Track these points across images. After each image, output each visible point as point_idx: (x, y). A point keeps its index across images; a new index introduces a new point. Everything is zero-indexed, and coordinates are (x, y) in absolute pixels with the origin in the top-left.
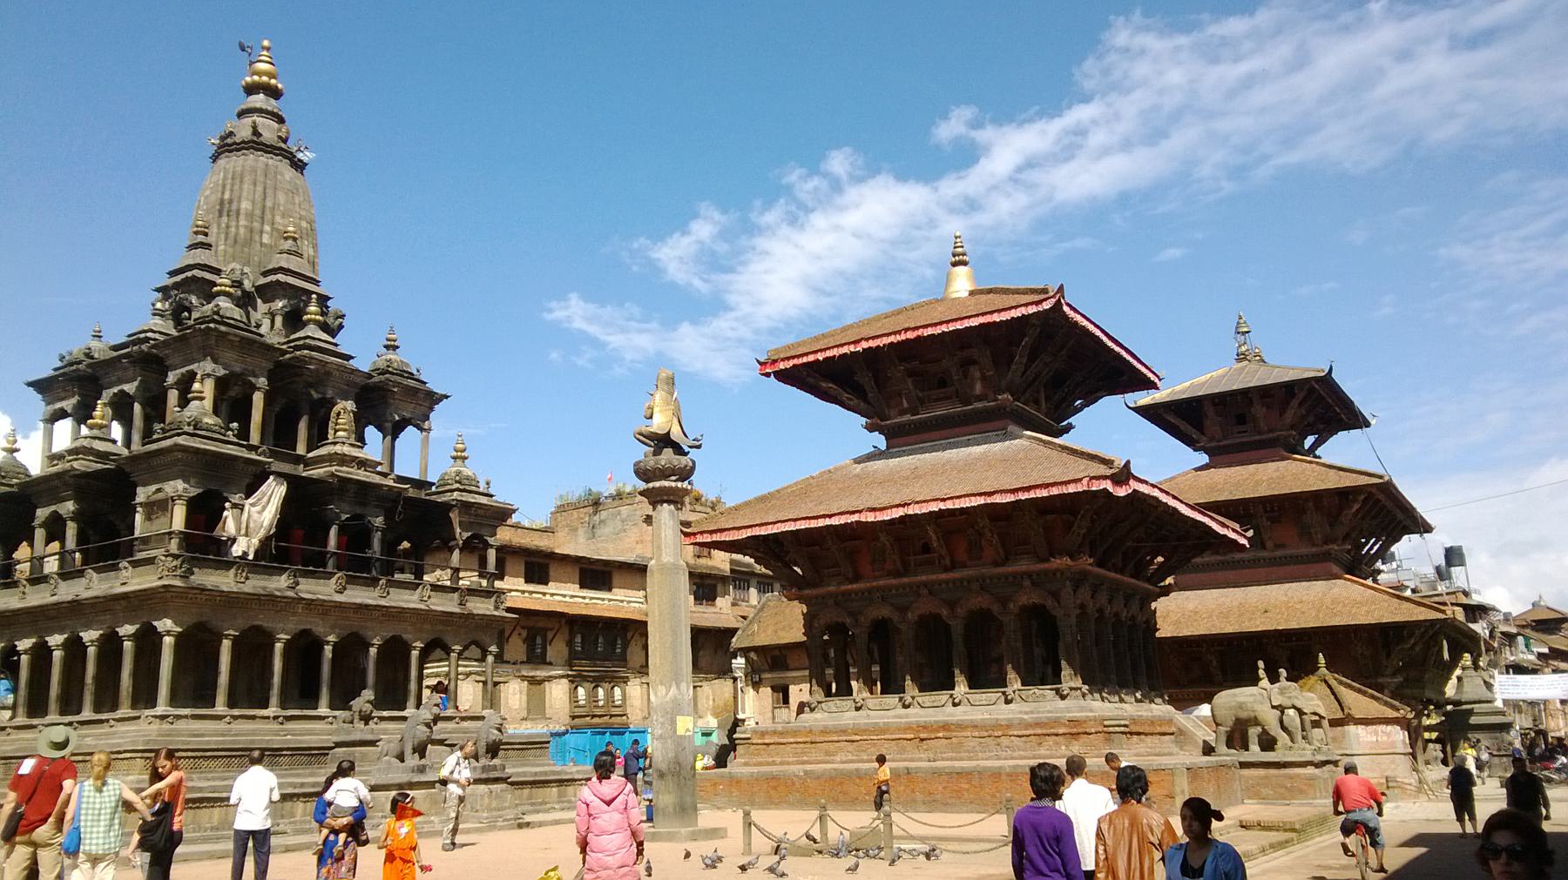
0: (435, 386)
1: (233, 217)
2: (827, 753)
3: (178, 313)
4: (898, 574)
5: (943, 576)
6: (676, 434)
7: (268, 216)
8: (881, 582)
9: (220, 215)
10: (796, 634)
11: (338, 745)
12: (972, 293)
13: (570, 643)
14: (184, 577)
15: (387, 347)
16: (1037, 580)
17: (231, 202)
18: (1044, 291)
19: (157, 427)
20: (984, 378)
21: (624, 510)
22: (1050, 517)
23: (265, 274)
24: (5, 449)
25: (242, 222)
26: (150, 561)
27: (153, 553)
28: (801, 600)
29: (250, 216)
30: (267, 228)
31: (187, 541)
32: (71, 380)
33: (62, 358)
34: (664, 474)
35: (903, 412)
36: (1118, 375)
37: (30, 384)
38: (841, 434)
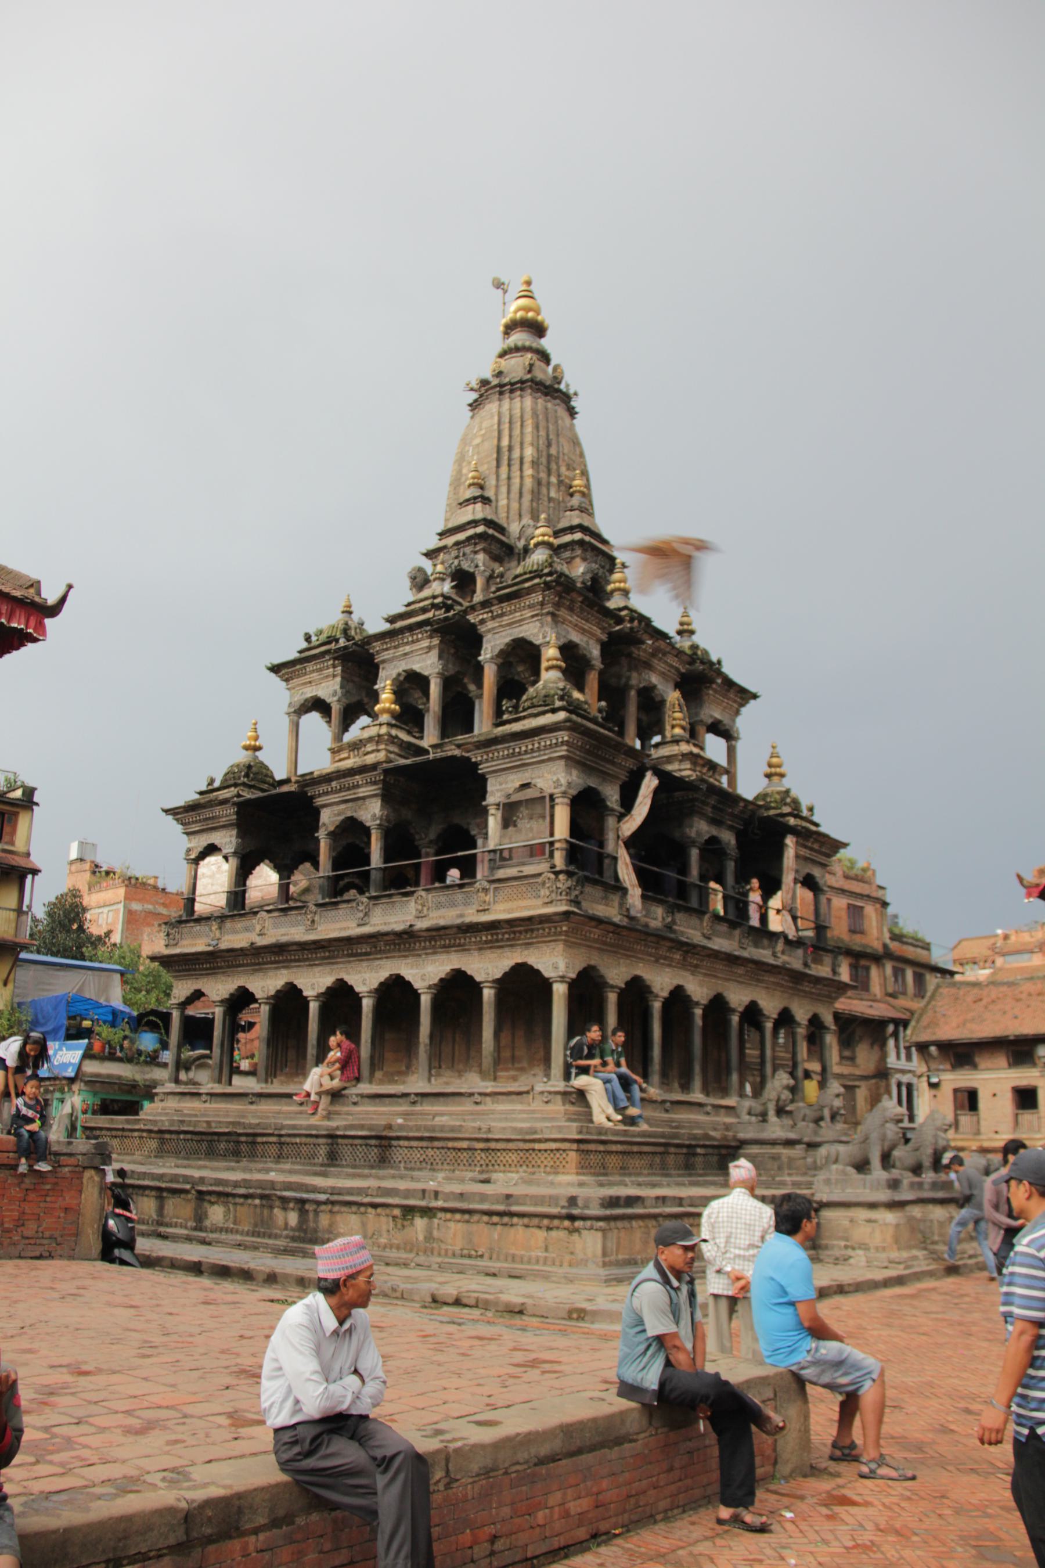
1: (516, 467)
7: (554, 466)
9: (498, 466)
14: (576, 902)
17: (510, 448)
19: (506, 704)
23: (557, 534)
24: (247, 748)
29: (535, 464)
30: (554, 480)
31: (573, 854)
33: (308, 638)
37: (275, 669)
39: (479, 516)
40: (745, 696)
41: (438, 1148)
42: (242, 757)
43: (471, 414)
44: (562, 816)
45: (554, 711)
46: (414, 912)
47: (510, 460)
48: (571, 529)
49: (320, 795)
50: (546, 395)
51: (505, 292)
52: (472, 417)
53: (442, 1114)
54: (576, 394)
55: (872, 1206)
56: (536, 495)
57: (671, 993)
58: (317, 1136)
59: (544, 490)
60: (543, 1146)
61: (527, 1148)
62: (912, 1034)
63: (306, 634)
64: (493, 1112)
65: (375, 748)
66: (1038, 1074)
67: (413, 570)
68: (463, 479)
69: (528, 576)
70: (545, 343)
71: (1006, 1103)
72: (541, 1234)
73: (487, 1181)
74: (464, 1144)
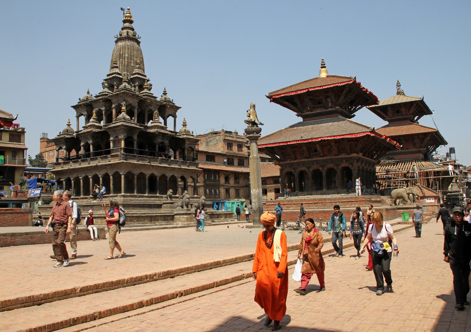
0: (177, 105)
2: (288, 207)
3: (111, 87)
4: (308, 158)
5: (320, 159)
6: (256, 122)
7: (132, 58)
8: (303, 160)
9: (120, 59)
10: (278, 174)
11: (164, 203)
12: (327, 76)
13: (204, 177)
16: (347, 160)
17: (122, 54)
18: (350, 78)
20: (332, 102)
21: (217, 138)
22: (351, 142)
23: (133, 75)
25: (126, 60)
26: (117, 156)
27: (117, 153)
28: (279, 165)
29: (128, 58)
30: (132, 61)
31: (125, 150)
32: (86, 106)
33: (80, 99)
34: (252, 132)
35: (308, 111)
36: (368, 99)
37: (72, 107)
38: (290, 117)
40: (179, 108)
42: (66, 127)
44: (123, 143)
48: (135, 74)
55: (183, 214)
56: (128, 66)
70: (133, 25)
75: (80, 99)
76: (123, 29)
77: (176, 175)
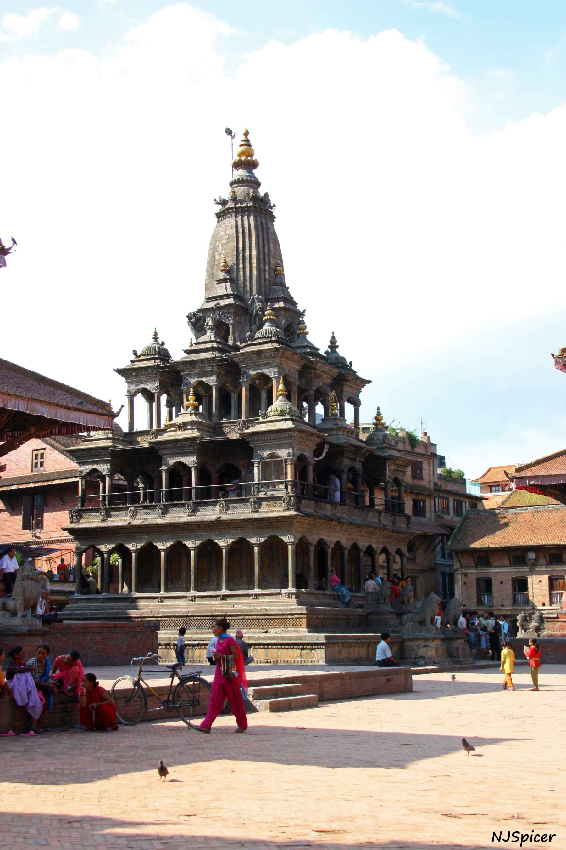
3: (221, 329)
7: (267, 260)
15: (329, 347)
27: (277, 494)
30: (267, 268)
33: (135, 353)
37: (121, 372)
39: (230, 292)
41: (241, 619)
43: (216, 219)
45: (286, 420)
46: (218, 511)
47: (244, 256)
49: (162, 449)
50: (261, 213)
51: (233, 138)
52: (218, 222)
53: (238, 604)
54: (274, 206)
57: (335, 544)
58: (178, 617)
59: (263, 275)
60: (252, 617)
61: (283, 618)
62: (451, 545)
63: (134, 351)
64: (263, 602)
65: (190, 427)
66: (528, 570)
67: (190, 313)
68: (216, 263)
69: (263, 340)
71: (508, 587)
72: (299, 651)
73: (267, 632)
74: (255, 617)
75: (135, 353)
76: (231, 184)
77: (374, 546)
